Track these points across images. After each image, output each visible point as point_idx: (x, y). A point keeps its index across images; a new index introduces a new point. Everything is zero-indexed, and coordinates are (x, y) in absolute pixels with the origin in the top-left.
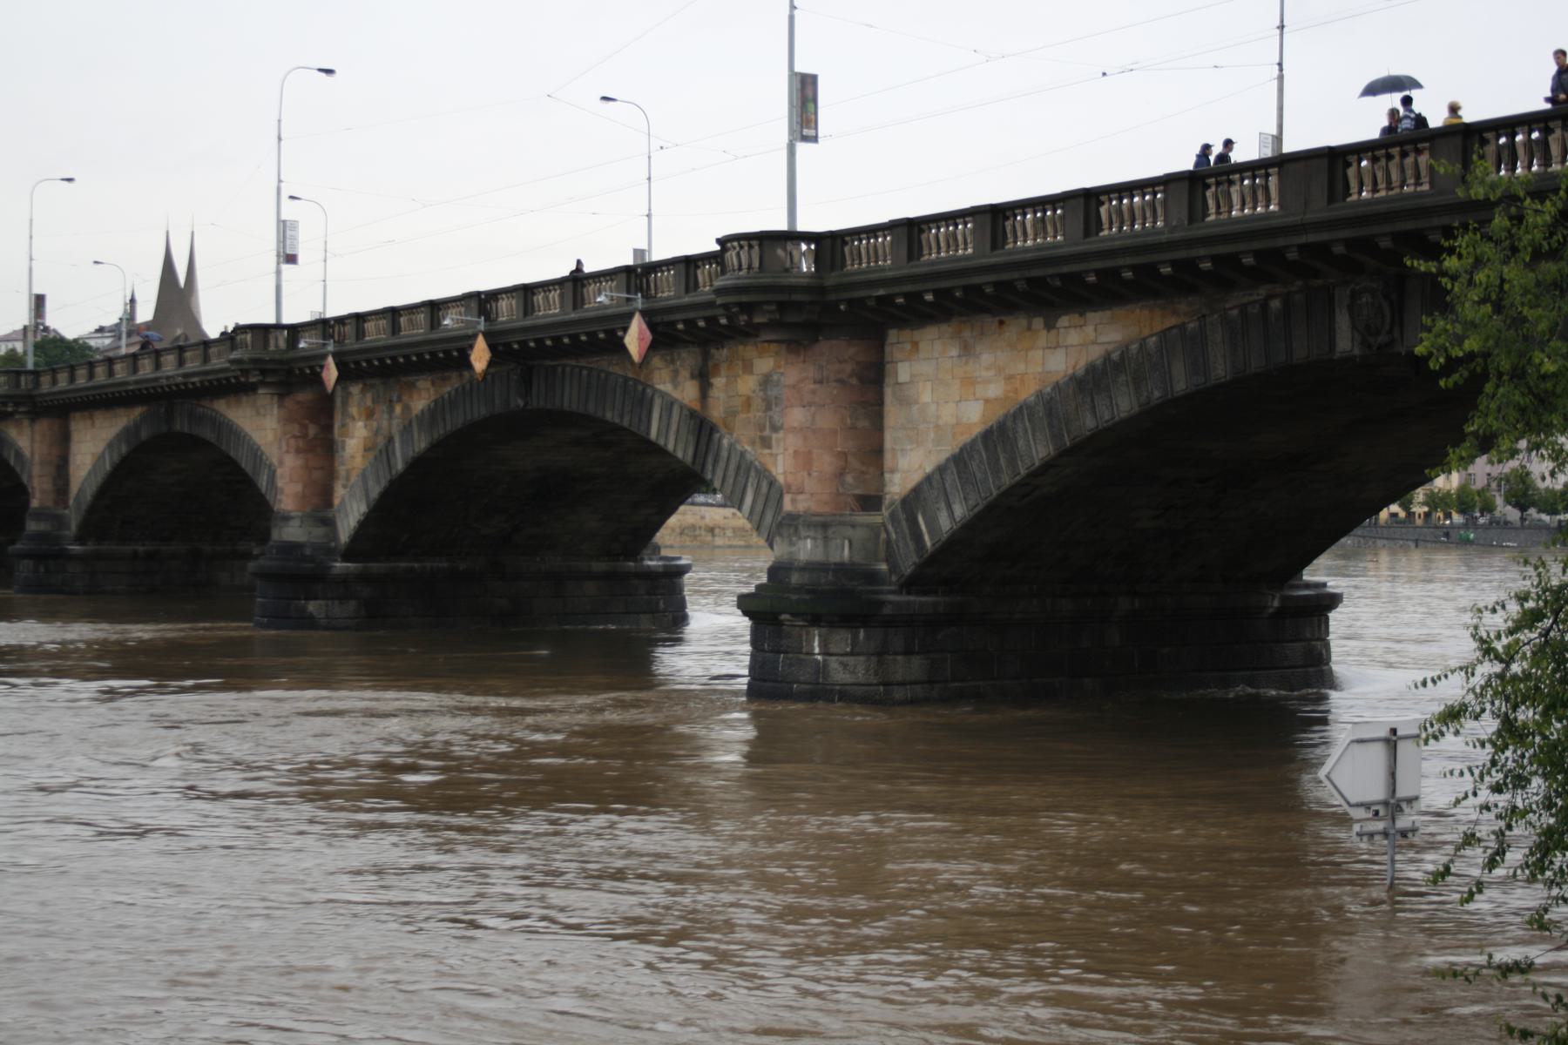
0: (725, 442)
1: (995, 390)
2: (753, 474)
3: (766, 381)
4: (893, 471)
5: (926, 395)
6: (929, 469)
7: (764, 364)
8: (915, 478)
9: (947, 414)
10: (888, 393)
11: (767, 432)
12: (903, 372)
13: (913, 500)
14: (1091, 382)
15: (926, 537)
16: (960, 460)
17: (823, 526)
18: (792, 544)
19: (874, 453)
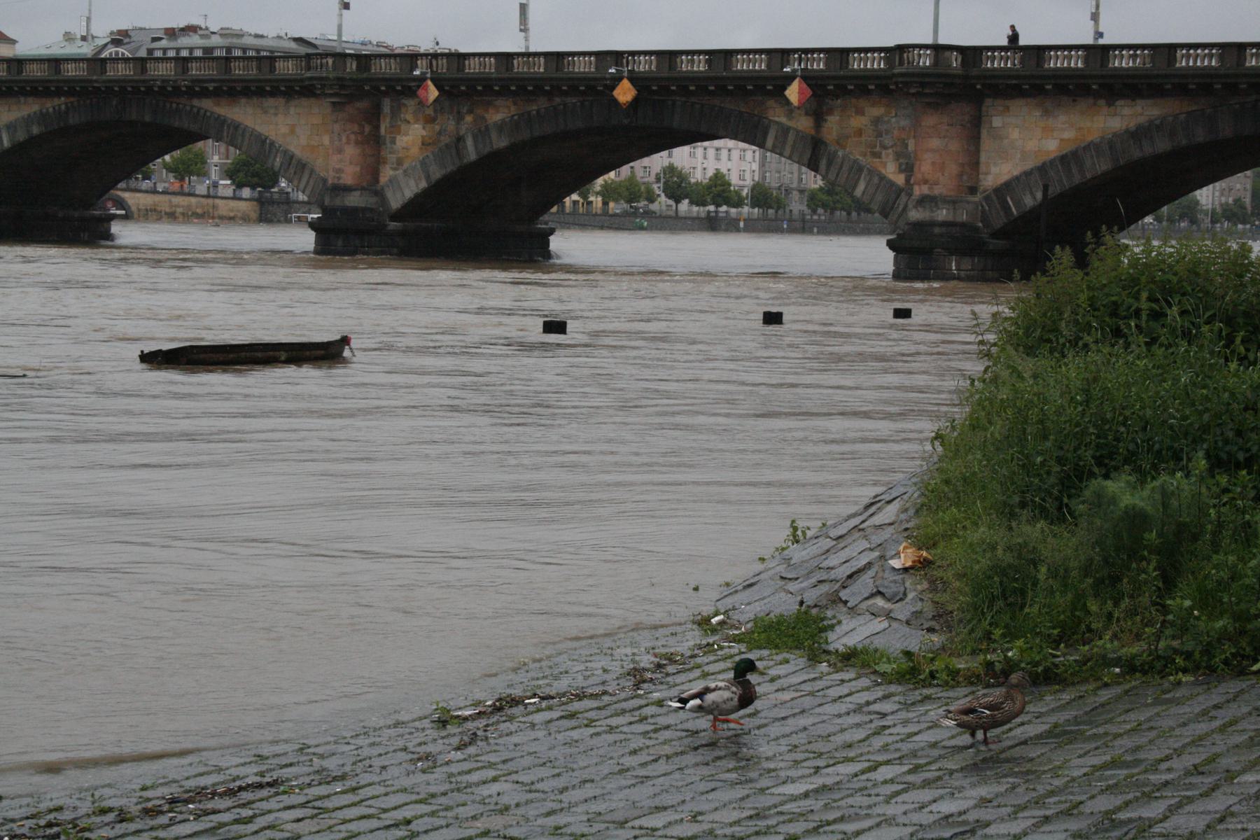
0: (840, 153)
1: (1068, 135)
2: (865, 172)
3: (877, 121)
4: (986, 174)
5: (1015, 134)
6: (1016, 173)
7: (877, 111)
8: (1005, 178)
9: (1032, 145)
10: (984, 133)
11: (878, 149)
12: (997, 122)
13: (1003, 191)
14: (1137, 134)
15: (1014, 209)
16: (1042, 169)
17: (953, 203)
18: (932, 211)
19: (975, 164)
